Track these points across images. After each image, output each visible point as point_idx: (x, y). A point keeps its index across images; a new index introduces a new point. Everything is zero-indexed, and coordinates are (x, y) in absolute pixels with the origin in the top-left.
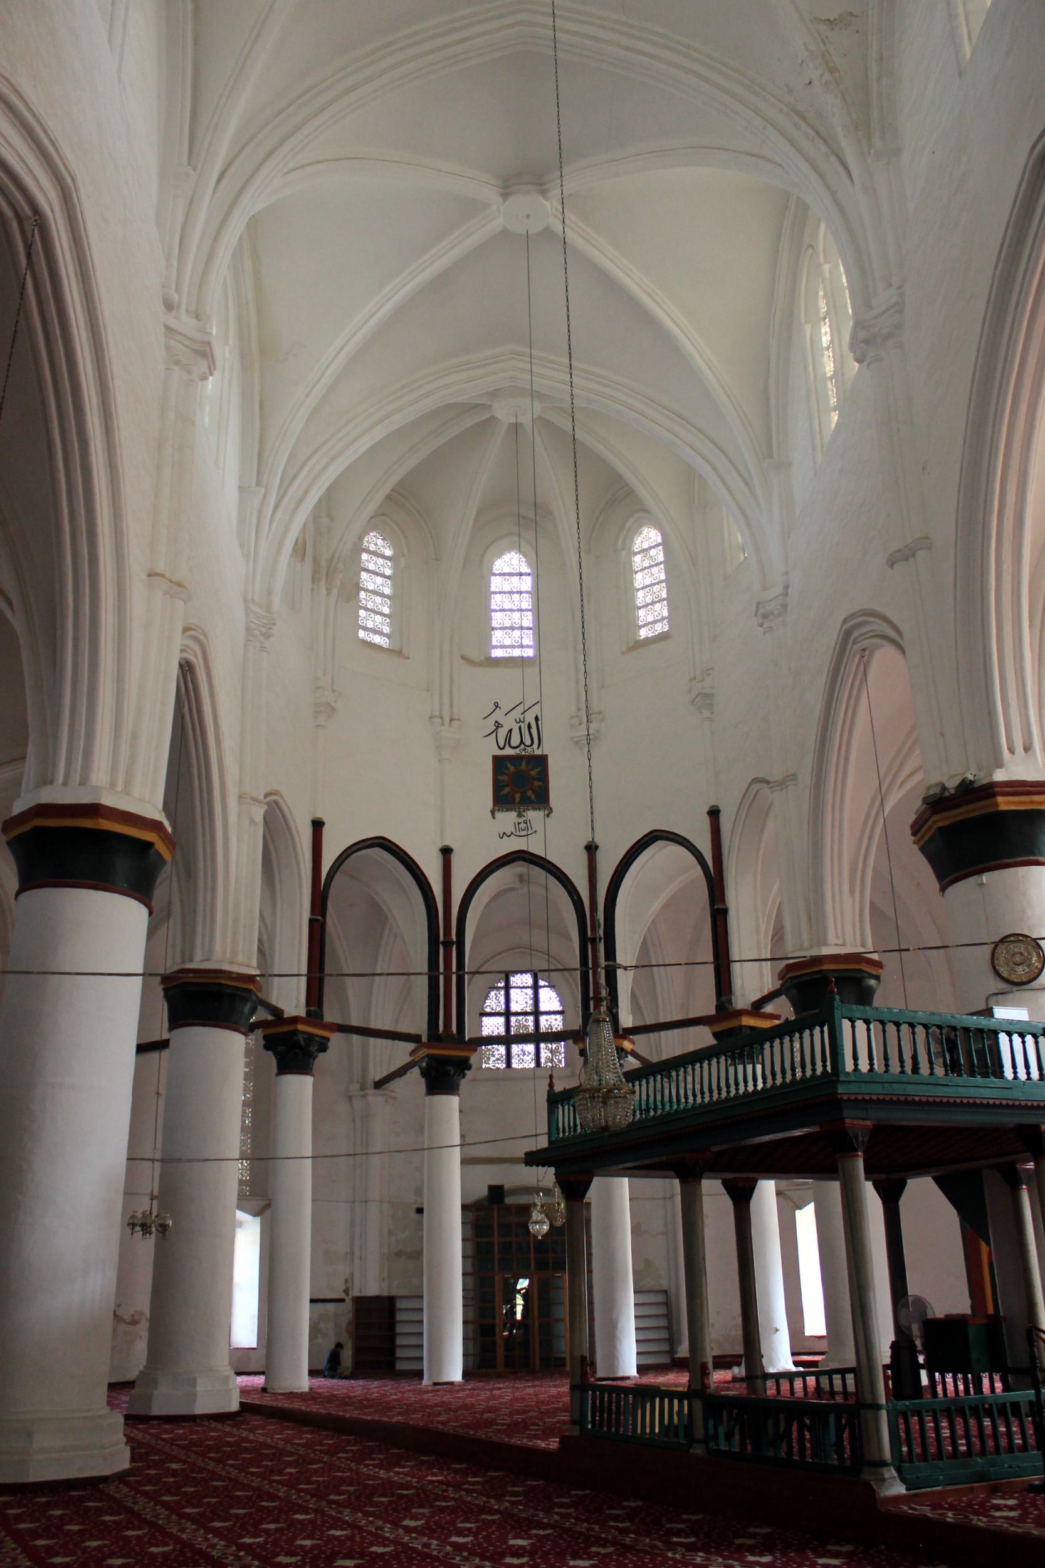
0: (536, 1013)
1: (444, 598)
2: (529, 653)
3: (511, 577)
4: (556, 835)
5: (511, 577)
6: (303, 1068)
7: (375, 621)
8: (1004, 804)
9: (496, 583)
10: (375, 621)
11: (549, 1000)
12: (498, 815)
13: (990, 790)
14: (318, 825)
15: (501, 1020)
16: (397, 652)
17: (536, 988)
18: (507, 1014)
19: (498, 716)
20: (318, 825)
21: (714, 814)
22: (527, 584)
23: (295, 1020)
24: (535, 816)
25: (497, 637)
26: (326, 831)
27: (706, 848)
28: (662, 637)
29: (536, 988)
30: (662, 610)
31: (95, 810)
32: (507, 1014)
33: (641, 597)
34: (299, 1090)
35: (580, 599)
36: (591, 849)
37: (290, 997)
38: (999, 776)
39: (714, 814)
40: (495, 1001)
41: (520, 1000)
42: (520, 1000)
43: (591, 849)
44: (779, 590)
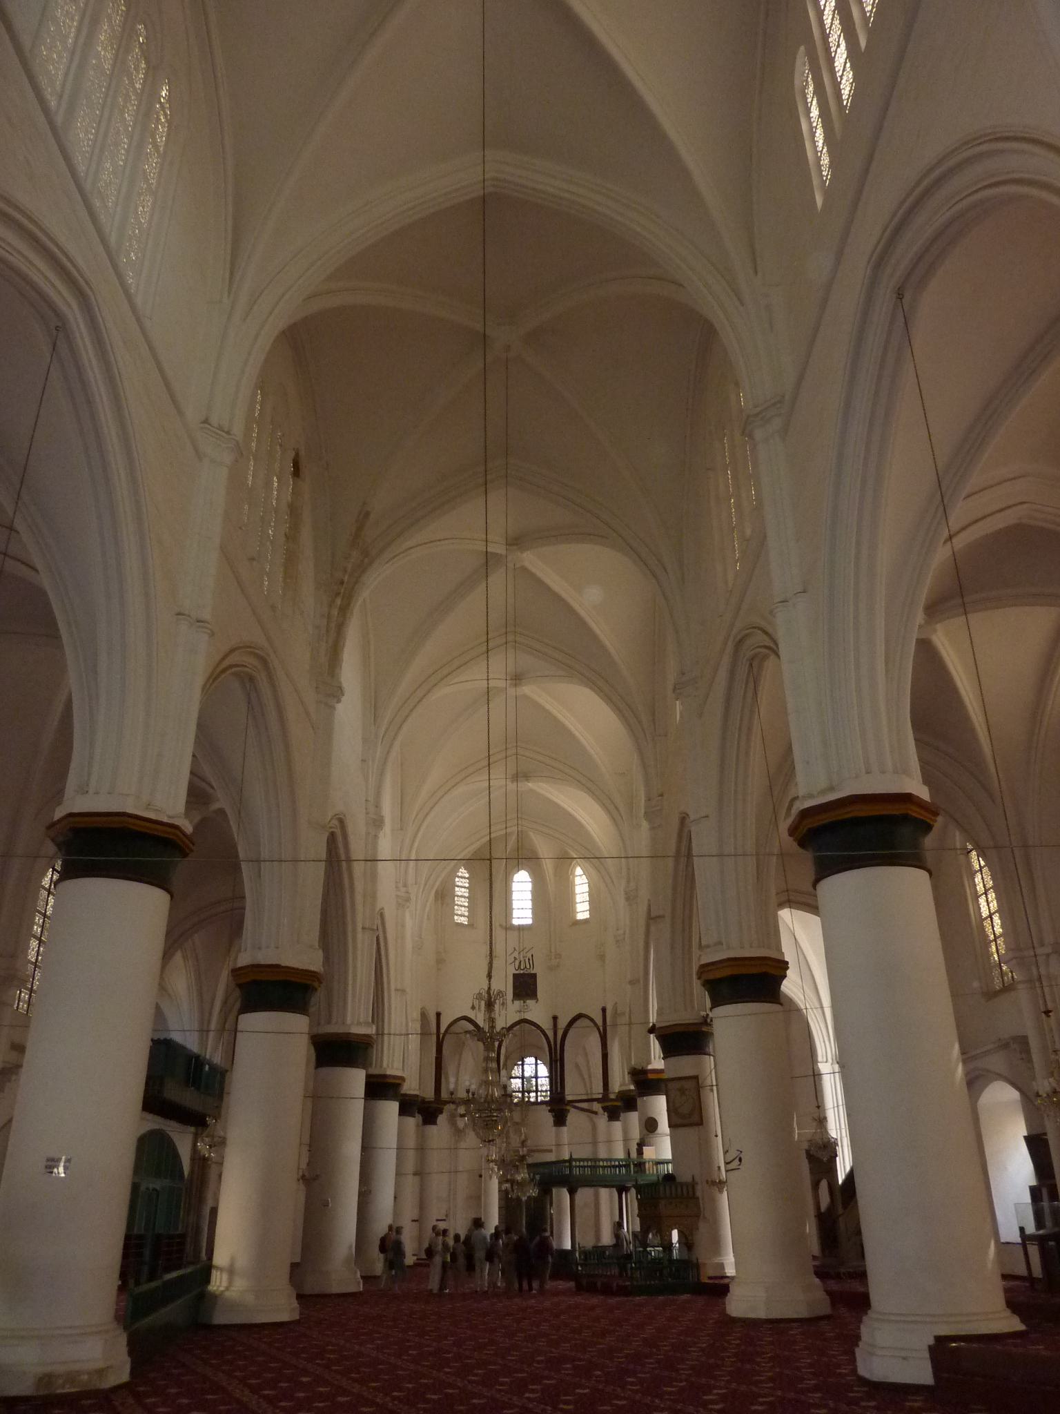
0: (536, 1077)
1: (492, 895)
2: (529, 922)
3: (522, 885)
4: (538, 1012)
5: (522, 885)
6: (434, 1123)
7: (461, 914)
8: (651, 1076)
9: (515, 887)
10: (461, 914)
11: (543, 1070)
12: (517, 1002)
13: (644, 1072)
14: (438, 1015)
15: (519, 1081)
16: (471, 925)
17: (536, 1064)
18: (523, 1078)
19: (516, 954)
20: (438, 1015)
21: (604, 1010)
22: (529, 886)
23: (430, 1102)
24: (530, 1002)
25: (515, 914)
26: (442, 1018)
27: (600, 1023)
28: (586, 921)
29: (536, 1064)
30: (586, 906)
31: (385, 1076)
32: (523, 1078)
33: (578, 899)
34: (432, 1129)
35: (551, 900)
36: (555, 1018)
37: (429, 1094)
38: (650, 1067)
39: (604, 1010)
40: (517, 1071)
41: (529, 1071)
42: (529, 1071)
43: (555, 1018)
44: (621, 932)
